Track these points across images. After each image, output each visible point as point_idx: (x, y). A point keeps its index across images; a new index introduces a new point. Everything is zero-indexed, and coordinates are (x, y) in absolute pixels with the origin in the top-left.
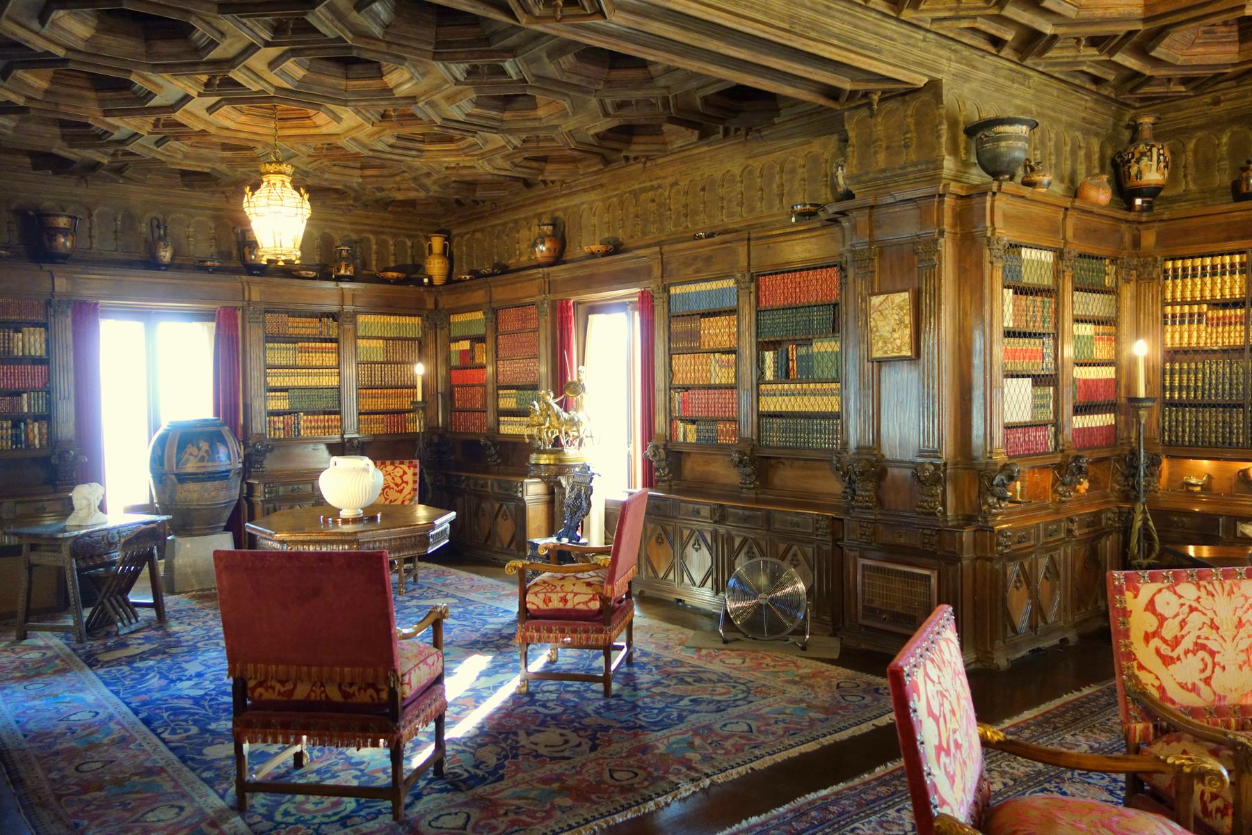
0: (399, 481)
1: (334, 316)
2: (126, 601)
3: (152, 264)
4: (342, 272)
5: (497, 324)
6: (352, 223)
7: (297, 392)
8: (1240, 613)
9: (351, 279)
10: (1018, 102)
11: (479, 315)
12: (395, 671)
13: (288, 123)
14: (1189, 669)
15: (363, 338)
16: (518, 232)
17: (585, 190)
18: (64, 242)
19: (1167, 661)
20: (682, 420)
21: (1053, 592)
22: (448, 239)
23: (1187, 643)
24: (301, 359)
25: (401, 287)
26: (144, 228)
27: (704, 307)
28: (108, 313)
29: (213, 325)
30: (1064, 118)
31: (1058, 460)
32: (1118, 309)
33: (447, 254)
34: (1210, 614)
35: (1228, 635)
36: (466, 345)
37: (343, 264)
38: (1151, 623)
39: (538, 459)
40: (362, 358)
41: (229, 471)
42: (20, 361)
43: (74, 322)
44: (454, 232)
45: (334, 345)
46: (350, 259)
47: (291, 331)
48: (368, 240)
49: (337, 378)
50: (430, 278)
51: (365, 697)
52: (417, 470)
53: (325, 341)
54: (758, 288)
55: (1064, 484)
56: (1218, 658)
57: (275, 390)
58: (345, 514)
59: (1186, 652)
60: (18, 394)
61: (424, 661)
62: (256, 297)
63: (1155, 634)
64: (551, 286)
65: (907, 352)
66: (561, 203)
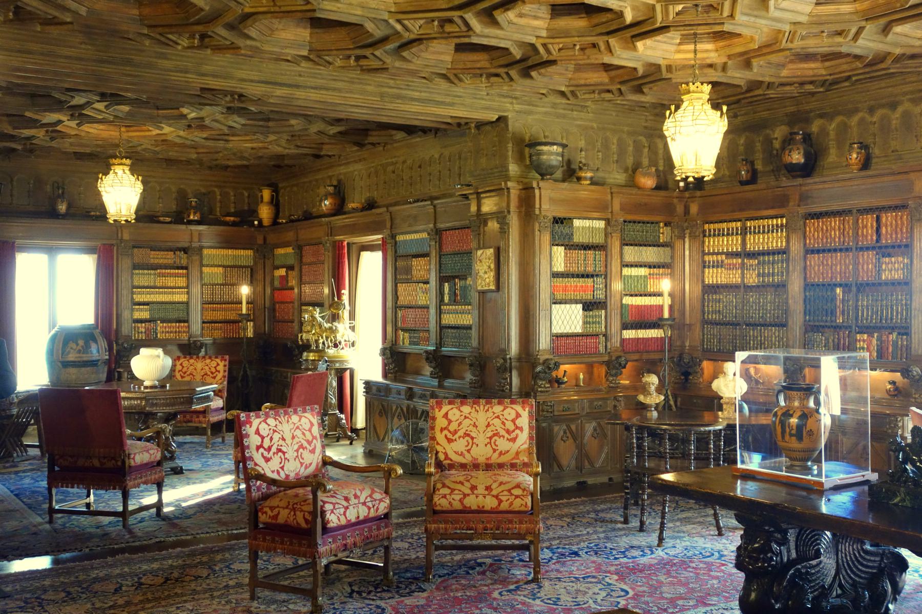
0: (213, 370)
1: (185, 250)
2: (22, 445)
3: (53, 214)
4: (192, 217)
5: (301, 257)
6: (201, 180)
7: (155, 306)
8: (489, 420)
9: (199, 223)
10: (579, 123)
11: (290, 250)
12: (124, 451)
13: (132, 129)
14: (460, 445)
15: (207, 266)
16: (319, 188)
17: (355, 162)
19: (450, 441)
20: (403, 330)
21: (601, 447)
23: (461, 433)
24: (160, 282)
25: (239, 227)
26: (48, 188)
27: (414, 251)
28: (23, 249)
29: (96, 256)
30: (626, 129)
31: (606, 358)
32: (672, 257)
33: (275, 203)
34: (474, 420)
35: (481, 430)
36: (282, 272)
37: (192, 211)
38: (444, 423)
39: (308, 356)
40: (206, 281)
41: (98, 361)
44: (280, 185)
45: (185, 271)
46: (196, 209)
47: (152, 261)
48: (214, 192)
49: (186, 296)
50: (260, 222)
51: (110, 464)
52: (227, 363)
53: (178, 268)
54: (440, 238)
55: (612, 376)
56: (475, 441)
57: (140, 304)
58: (147, 383)
59: (460, 437)
61: (148, 451)
63: (445, 429)
64: (332, 232)
65: (493, 287)
66: (343, 170)
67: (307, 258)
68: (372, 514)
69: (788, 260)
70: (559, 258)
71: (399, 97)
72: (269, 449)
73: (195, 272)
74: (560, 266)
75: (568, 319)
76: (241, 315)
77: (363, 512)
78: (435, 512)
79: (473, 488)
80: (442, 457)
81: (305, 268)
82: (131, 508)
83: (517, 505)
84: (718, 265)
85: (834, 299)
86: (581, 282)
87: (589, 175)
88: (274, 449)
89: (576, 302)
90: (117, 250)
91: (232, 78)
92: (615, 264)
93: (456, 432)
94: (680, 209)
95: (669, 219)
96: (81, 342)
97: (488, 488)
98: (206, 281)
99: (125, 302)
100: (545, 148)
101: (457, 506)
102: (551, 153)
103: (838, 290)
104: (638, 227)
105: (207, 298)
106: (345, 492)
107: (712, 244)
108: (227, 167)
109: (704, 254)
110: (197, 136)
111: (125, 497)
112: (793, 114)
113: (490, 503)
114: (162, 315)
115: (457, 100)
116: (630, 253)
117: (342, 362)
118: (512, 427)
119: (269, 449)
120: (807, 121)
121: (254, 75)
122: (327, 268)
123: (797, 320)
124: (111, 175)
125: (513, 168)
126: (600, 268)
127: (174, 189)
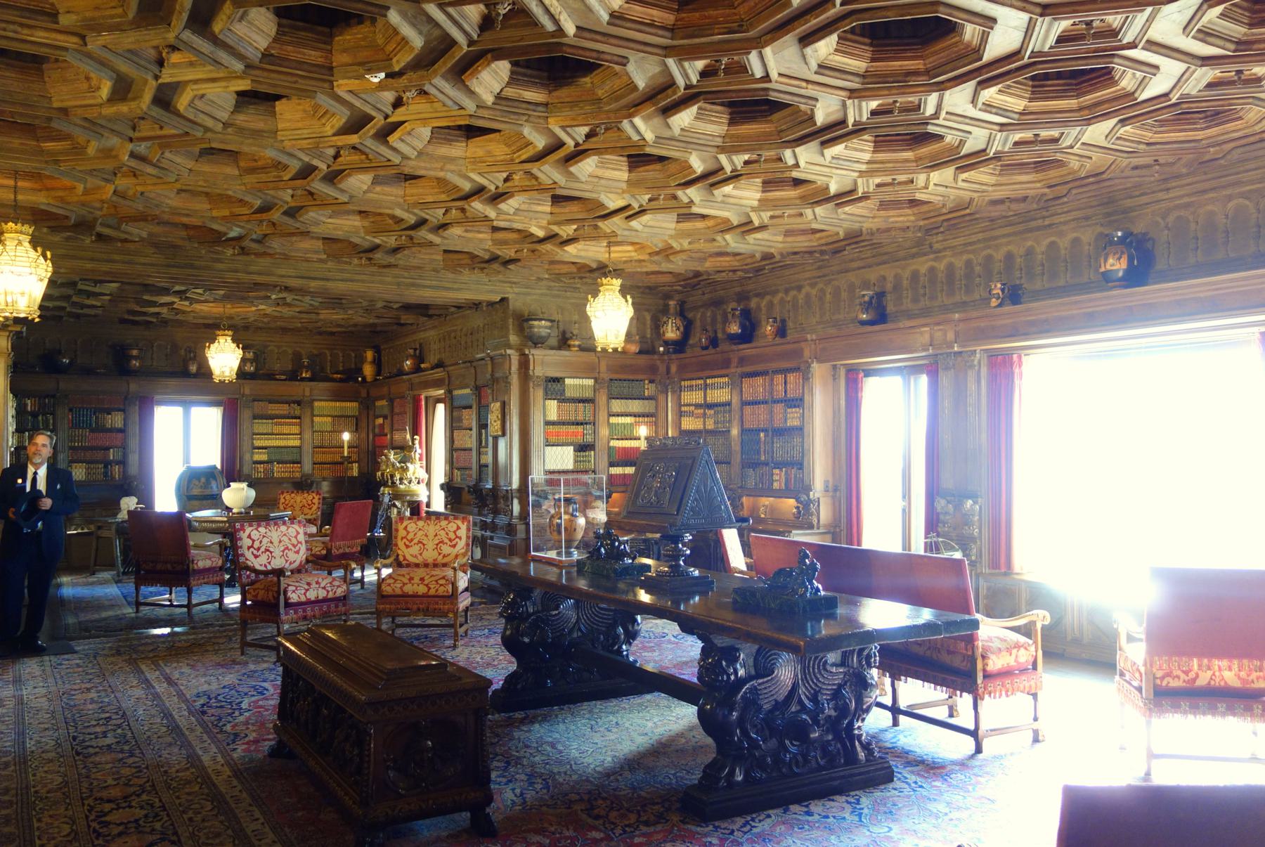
9: (310, 380)
18: (136, 363)
19: (407, 547)
22: (377, 350)
24: (277, 429)
25: (347, 382)
26: (182, 352)
28: (161, 403)
33: (378, 363)
40: (316, 428)
42: (111, 430)
43: (140, 408)
46: (308, 368)
60: (108, 449)
62: (247, 391)
66: (422, 335)
67: (397, 410)
68: (331, 595)
69: (730, 411)
70: (553, 409)
71: (413, 285)
72: (258, 549)
73: (307, 420)
74: (553, 415)
75: (562, 458)
76: (343, 457)
77: (322, 594)
78: (383, 596)
79: (411, 579)
80: (401, 558)
81: (396, 417)
82: (194, 602)
83: (441, 591)
84: (691, 414)
85: (759, 442)
86: (572, 429)
87: (577, 343)
88: (263, 549)
89: (567, 444)
90: (233, 401)
91: (273, 275)
92: (602, 415)
93: (412, 540)
94: (662, 369)
95: (652, 377)
96: (203, 480)
97: (422, 579)
98: (316, 428)
99: (246, 446)
100: (536, 323)
101: (398, 592)
102: (540, 327)
103: (762, 435)
104: (625, 384)
105: (317, 443)
106: (309, 580)
107: (687, 397)
108: (332, 334)
109: (681, 406)
110: (286, 311)
111: (190, 592)
112: (739, 294)
113: (422, 589)
114: (278, 457)
115: (463, 286)
116: (617, 405)
117: (412, 495)
118: (453, 536)
119: (258, 549)
120: (748, 299)
121: (291, 272)
122: (408, 418)
123: (737, 459)
124: (216, 344)
125: (513, 339)
126: (589, 417)
127: (290, 351)
